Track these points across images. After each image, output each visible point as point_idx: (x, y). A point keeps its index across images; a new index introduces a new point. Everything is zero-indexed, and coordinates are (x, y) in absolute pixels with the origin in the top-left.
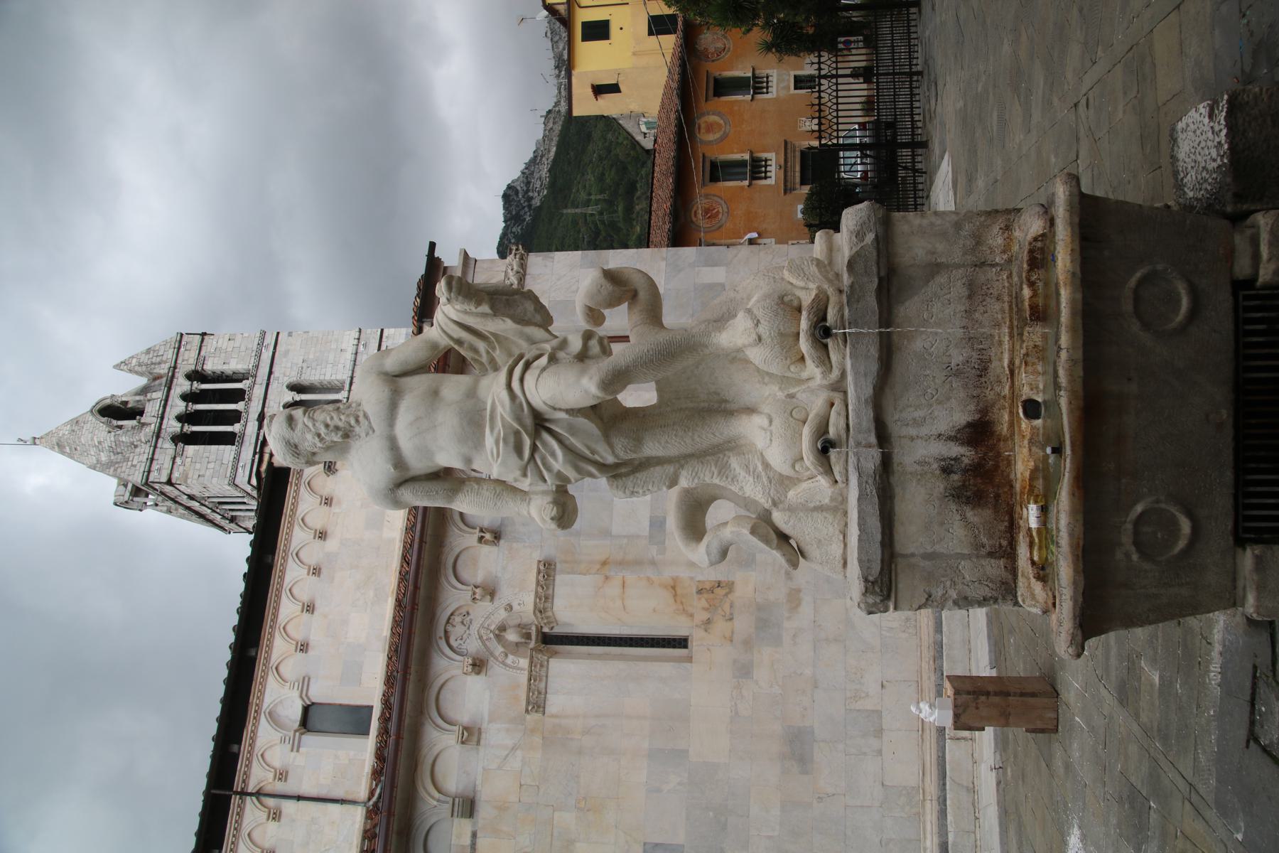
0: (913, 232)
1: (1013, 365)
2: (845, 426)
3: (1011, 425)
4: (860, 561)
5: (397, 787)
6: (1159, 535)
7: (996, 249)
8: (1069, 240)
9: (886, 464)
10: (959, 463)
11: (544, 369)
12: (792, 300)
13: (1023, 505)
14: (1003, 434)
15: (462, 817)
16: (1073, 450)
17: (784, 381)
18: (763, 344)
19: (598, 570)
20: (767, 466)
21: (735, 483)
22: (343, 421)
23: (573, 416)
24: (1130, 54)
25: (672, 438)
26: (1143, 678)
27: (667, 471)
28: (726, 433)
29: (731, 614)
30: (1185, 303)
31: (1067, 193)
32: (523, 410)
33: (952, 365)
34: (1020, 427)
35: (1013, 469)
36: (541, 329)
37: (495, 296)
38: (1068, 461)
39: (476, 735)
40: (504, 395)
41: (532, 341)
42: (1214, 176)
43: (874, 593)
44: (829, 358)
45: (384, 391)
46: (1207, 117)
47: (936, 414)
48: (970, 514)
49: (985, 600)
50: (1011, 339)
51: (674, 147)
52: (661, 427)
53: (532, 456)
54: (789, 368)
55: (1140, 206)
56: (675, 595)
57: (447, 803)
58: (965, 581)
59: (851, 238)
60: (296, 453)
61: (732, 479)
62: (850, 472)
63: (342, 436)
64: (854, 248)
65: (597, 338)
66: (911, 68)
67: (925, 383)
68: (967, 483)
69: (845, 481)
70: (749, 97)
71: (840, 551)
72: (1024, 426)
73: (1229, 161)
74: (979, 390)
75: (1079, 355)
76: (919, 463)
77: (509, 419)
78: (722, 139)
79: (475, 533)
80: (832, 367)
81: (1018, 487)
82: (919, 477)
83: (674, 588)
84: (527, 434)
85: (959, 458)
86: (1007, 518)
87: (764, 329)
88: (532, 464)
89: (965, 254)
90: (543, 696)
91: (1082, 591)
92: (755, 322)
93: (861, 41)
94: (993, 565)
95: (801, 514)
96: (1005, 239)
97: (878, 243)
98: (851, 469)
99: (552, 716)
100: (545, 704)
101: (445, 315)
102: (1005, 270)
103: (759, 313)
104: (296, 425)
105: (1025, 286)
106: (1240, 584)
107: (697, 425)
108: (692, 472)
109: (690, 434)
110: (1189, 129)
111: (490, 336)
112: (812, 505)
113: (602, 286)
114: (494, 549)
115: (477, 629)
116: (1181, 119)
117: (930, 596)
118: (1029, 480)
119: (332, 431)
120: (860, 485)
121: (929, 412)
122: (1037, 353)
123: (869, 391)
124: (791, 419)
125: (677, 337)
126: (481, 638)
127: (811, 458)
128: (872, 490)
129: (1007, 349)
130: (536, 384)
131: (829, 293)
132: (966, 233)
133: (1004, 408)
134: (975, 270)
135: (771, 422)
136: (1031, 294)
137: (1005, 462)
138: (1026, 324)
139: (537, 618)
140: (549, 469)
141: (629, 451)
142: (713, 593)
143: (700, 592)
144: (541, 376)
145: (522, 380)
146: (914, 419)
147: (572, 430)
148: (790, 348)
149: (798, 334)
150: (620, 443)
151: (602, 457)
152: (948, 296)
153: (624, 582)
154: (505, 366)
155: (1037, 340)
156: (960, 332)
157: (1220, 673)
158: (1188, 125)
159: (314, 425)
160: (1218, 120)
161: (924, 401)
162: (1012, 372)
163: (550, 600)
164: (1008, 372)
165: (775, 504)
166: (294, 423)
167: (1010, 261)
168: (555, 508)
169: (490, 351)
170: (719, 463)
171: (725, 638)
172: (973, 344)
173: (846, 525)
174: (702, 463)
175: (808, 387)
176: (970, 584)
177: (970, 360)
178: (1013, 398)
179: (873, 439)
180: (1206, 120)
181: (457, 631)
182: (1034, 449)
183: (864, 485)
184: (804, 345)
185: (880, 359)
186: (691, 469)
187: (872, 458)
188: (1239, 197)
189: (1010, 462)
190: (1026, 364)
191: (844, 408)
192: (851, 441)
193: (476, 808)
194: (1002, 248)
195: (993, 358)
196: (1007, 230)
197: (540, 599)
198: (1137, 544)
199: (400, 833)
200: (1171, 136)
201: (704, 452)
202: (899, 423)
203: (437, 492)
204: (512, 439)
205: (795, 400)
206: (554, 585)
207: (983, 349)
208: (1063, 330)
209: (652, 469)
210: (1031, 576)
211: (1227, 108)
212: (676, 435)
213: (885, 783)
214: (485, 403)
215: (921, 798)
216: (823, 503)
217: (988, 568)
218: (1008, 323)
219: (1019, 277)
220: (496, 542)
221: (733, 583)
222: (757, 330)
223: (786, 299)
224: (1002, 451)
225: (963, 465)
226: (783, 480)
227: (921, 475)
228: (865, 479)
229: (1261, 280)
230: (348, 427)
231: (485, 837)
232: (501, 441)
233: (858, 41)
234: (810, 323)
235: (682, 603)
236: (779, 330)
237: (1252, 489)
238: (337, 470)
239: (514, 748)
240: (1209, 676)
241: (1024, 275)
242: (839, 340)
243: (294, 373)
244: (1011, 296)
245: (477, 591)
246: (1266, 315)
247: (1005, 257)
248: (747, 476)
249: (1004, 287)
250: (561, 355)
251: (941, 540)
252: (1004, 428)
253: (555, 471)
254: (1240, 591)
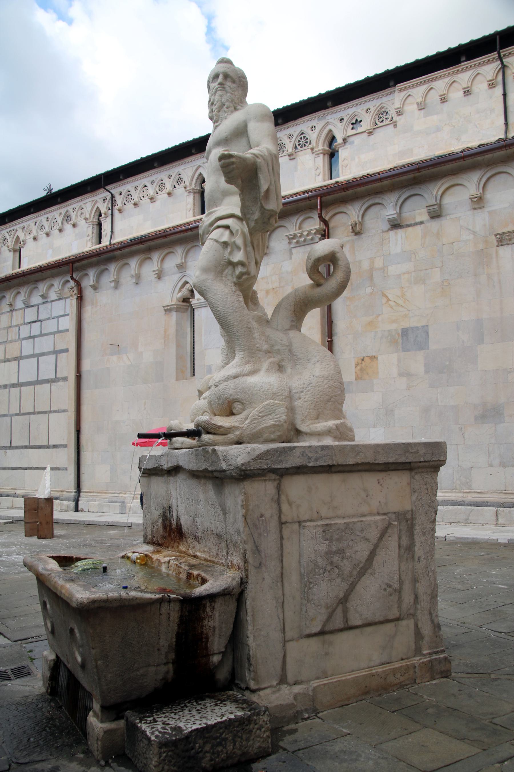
2: (176, 447)
5: (435, 168)
11: (216, 241)
15: (428, 213)
39: (479, 206)
57: (436, 201)
64: (221, 453)
65: (244, 270)
90: (509, 242)
92: (216, 384)
99: (497, 252)
100: (504, 245)
103: (221, 387)
104: (215, 82)
107: (231, 348)
125: (235, 328)
131: (229, 435)
145: (219, 227)
166: (216, 79)
193: (436, 219)
199: (415, 178)
213: (472, 469)
214: (220, 205)
215: (465, 491)
222: (213, 386)
223: (236, 404)
231: (421, 229)
239: (474, 233)
250: (229, 249)
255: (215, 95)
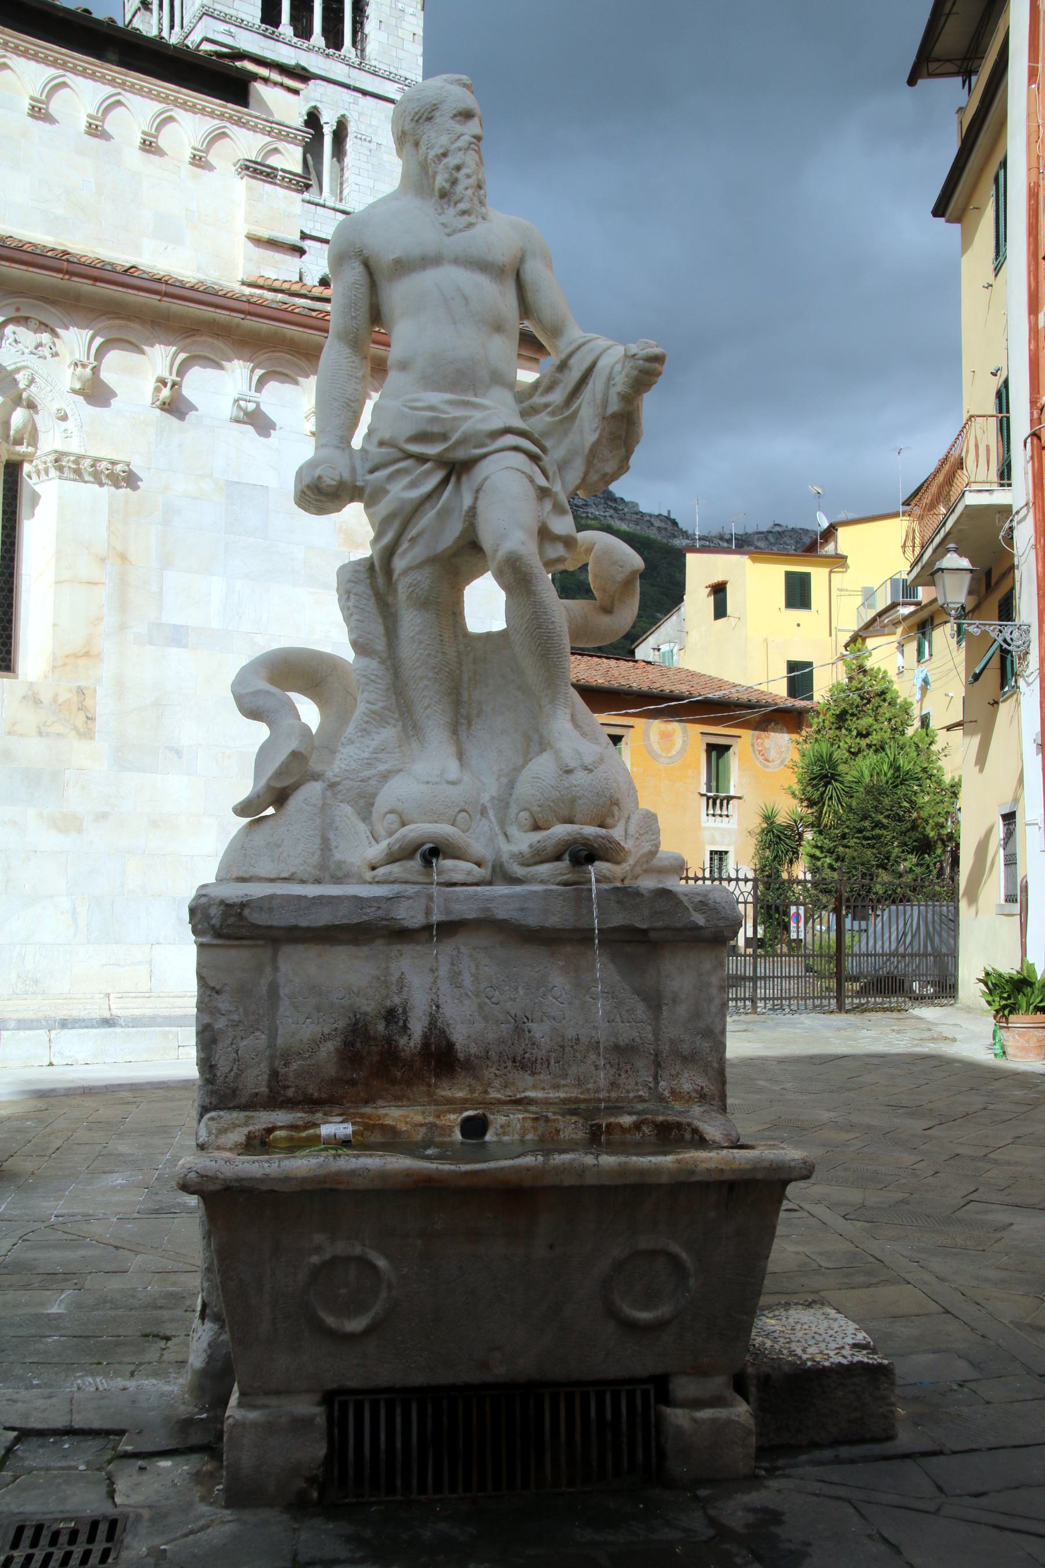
0: (701, 975)
1: (528, 1104)
2: (454, 881)
3: (450, 1101)
4: (272, 897)
6: (343, 1291)
7: (676, 1082)
8: (735, 1166)
9: (401, 934)
10: (399, 1032)
12: (613, 816)
13: (346, 1118)
14: (438, 1090)
16: (467, 1173)
17: (503, 803)
18: (561, 775)
19: (114, 548)
20: (385, 776)
21: (359, 734)
22: (464, 192)
23: (466, 516)
24: (872, 1260)
25: (425, 649)
26: (49, 1293)
27: (378, 641)
28: (430, 723)
29: (48, 735)
30: (644, 1316)
31: (793, 1164)
32: (475, 447)
33: (530, 1024)
34: (450, 1112)
35: (391, 1104)
36: (580, 481)
37: (625, 421)
38: (453, 1167)
40: (497, 424)
41: (563, 466)
42: (785, 1352)
43: (225, 916)
44: (542, 862)
45: (503, 255)
46: (854, 1341)
47: (467, 1002)
48: (330, 1046)
49: (212, 1067)
50: (561, 1100)
51: (645, 688)
52: (441, 636)
53: (409, 456)
54: (525, 809)
55: (768, 1257)
56: (76, 656)
58: (239, 1039)
59: (698, 894)
60: (420, 118)
61: (365, 730)
62: (391, 885)
63: (443, 188)
66: (761, 999)
67: (507, 988)
68: (373, 1043)
69: (377, 879)
70: (704, 792)
71: (263, 873)
72: (452, 1117)
73: (809, 1368)
74: (495, 1058)
75: (590, 1180)
76: (401, 978)
77: (465, 427)
78: (651, 752)
79: (171, 374)
80: (529, 865)
81: (367, 1110)
82: (383, 978)
83: (87, 654)
84: (446, 450)
85: (405, 1032)
86: (324, 1096)
87: (580, 778)
88: (401, 455)
89: (672, 1042)
91: (276, 1189)
92: (590, 767)
93: (798, 935)
94: (260, 1078)
95: (318, 821)
96: (688, 1093)
97: (690, 929)
98: (397, 888)
101: (605, 351)
102: (650, 1093)
104: (459, 122)
105: (634, 1118)
106: (273, 1401)
108: (376, 675)
109: (430, 675)
110: (831, 1322)
111: (571, 410)
112: (331, 835)
113: (621, 567)
114: (149, 398)
115: (29, 364)
116: (839, 1313)
117: (217, 992)
118: (382, 1125)
119: (451, 174)
120: (376, 899)
121: (470, 993)
122: (550, 1133)
123: (501, 913)
124: (457, 810)
126: (18, 370)
127: (412, 835)
128: (369, 915)
129: (548, 1095)
130: (513, 468)
132: (698, 1043)
133: (472, 1091)
134: (651, 1054)
135: (453, 783)
136: (626, 1126)
137: (399, 1093)
138: (586, 1119)
139: (48, 454)
140: (391, 478)
141: (411, 589)
142: (79, 709)
143: (81, 691)
144: (524, 476)
145: (516, 449)
146: (460, 973)
147: (445, 514)
148: (555, 811)
149: (572, 822)
150: (424, 578)
151: (404, 552)
152: (618, 1019)
153: (96, 584)
154: (528, 425)
155: (566, 1134)
156: (570, 1033)
157: (97, 1389)
158: (836, 1320)
159: (460, 150)
160: (856, 1354)
161: (482, 986)
162: (518, 1102)
163: (72, 476)
164: (518, 1096)
165: (332, 785)
166: (462, 119)
167: (661, 1099)
168: (334, 483)
169: (549, 409)
170: (387, 712)
171: (14, 725)
172: (555, 1051)
173: (303, 882)
174: (387, 690)
175: (497, 835)
176: (234, 1046)
177: (535, 1047)
178: (484, 1104)
179: (435, 918)
180: (851, 1342)
181: (27, 337)
182: (423, 1130)
183: (376, 904)
184: (561, 831)
185: (542, 929)
186: (379, 673)
187: (410, 915)
188: (765, 1381)
189: (398, 1099)
190: (535, 1119)
191: (475, 881)
192: (435, 889)
194: (678, 1090)
195: (537, 1077)
196: (701, 1096)
197: (74, 462)
198: (333, 1261)
200: (814, 1302)
201: (401, 693)
202: (455, 953)
203: (353, 318)
204: (436, 429)
205: (479, 816)
206: (93, 483)
207: (549, 1064)
208: (622, 1159)
209: (381, 621)
210: (251, 1128)
211: (873, 1364)
212: (429, 655)
216: (335, 851)
217: (256, 1071)
218: (582, 1097)
219: (643, 1110)
220: (158, 403)
221: (92, 738)
222: (579, 769)
224: (415, 1089)
225: (397, 1037)
226: (364, 797)
227: (386, 981)
228: (384, 906)
229: (669, 1411)
230: (455, 198)
232: (434, 414)
233: (798, 932)
234: (591, 838)
235: (65, 665)
236: (580, 799)
237: (398, 1411)
238: (242, 178)
240: (87, 1376)
241: (649, 1117)
242: (568, 876)
243: (363, 129)
244: (617, 1100)
245: (88, 371)
246: (624, 1419)
247: (667, 1094)
248: (371, 750)
249: (628, 1092)
250: (548, 505)
251: (296, 1007)
252: (446, 1091)
253: (388, 487)
254: (260, 1401)
255: (465, 153)
